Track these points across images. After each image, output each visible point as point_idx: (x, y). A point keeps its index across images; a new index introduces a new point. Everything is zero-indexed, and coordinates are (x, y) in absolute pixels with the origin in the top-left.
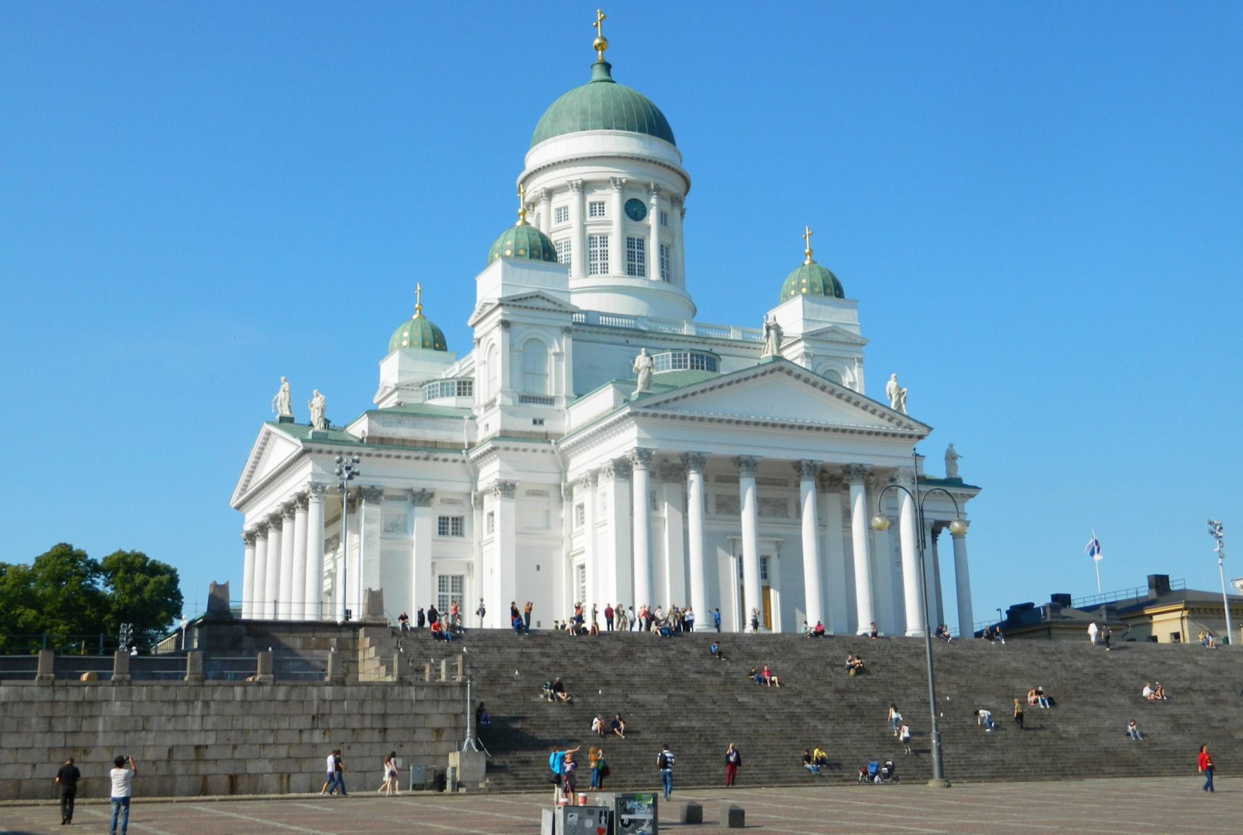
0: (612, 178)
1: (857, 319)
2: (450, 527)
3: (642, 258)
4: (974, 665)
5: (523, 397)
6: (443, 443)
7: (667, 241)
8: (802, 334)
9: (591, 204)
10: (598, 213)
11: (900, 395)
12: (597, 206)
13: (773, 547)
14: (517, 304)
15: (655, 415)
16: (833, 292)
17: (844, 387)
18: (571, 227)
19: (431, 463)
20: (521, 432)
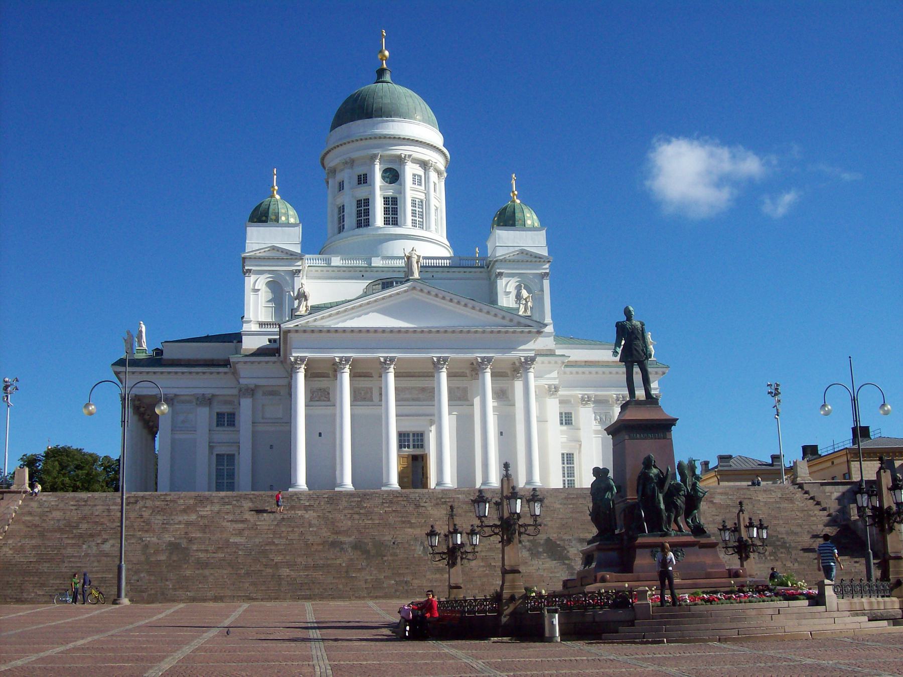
1: (546, 243)
3: (395, 211)
6: (218, 360)
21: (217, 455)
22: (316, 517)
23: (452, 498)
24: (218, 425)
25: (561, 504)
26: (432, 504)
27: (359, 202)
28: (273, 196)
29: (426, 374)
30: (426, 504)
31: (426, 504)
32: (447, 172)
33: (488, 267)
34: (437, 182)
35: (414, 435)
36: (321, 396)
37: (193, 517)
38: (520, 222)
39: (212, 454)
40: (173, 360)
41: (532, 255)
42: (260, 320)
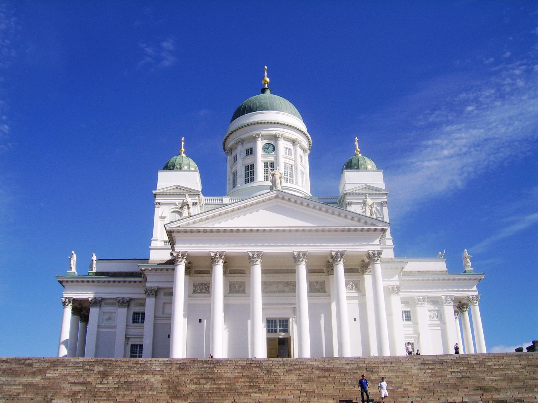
1: (383, 181)
10: (249, 154)
21: (132, 345)
24: (134, 322)
25: (418, 369)
26: (285, 370)
27: (247, 168)
28: (180, 154)
29: (290, 271)
30: (278, 371)
31: (278, 371)
32: (310, 150)
34: (303, 156)
35: (280, 321)
37: (38, 380)
38: (363, 166)
39: (128, 344)
41: (372, 188)
42: (164, 239)
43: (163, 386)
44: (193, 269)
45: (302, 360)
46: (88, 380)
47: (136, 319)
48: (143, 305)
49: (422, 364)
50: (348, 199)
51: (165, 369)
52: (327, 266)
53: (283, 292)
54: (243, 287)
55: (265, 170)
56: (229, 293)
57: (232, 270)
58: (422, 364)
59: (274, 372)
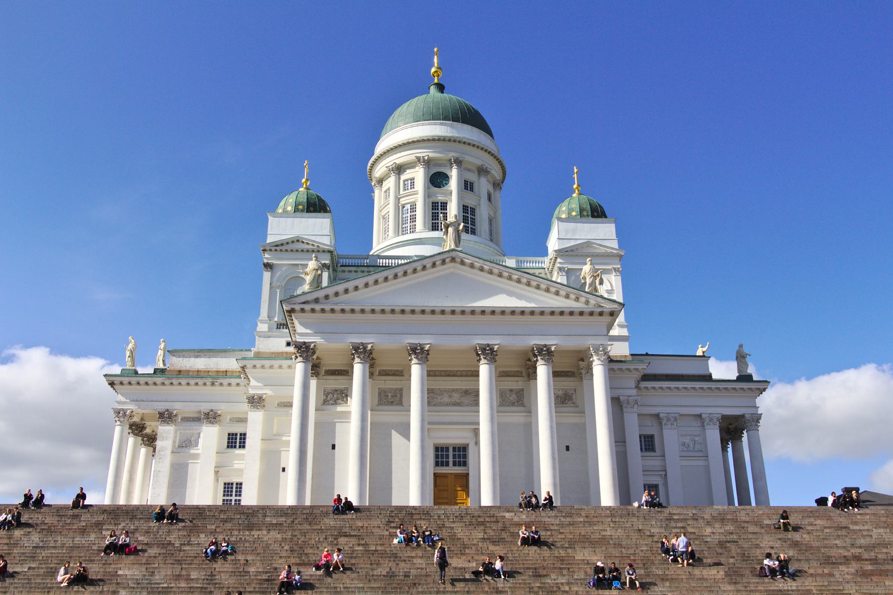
0: (418, 159)
2: (236, 441)
4: (549, 533)
5: (281, 324)
6: (232, 372)
7: (471, 203)
8: (555, 251)
9: (404, 181)
11: (595, 277)
12: (409, 181)
13: (471, 435)
14: (278, 248)
15: (313, 310)
16: (590, 213)
17: (602, 297)
18: (389, 204)
19: (217, 388)
20: (272, 353)
22: (281, 540)
23: (493, 516)
24: (228, 447)
31: (452, 525)
33: (548, 269)
36: (338, 399)
39: (217, 480)
40: (180, 371)
43: (283, 547)
44: (324, 369)
45: (488, 510)
46: (168, 539)
47: (232, 442)
48: (243, 420)
49: (667, 519)
50: (560, 263)
51: (285, 521)
52: (528, 367)
53: (459, 404)
54: (398, 396)
55: (433, 213)
56: (379, 404)
57: (383, 370)
58: (667, 519)
59: (447, 527)
